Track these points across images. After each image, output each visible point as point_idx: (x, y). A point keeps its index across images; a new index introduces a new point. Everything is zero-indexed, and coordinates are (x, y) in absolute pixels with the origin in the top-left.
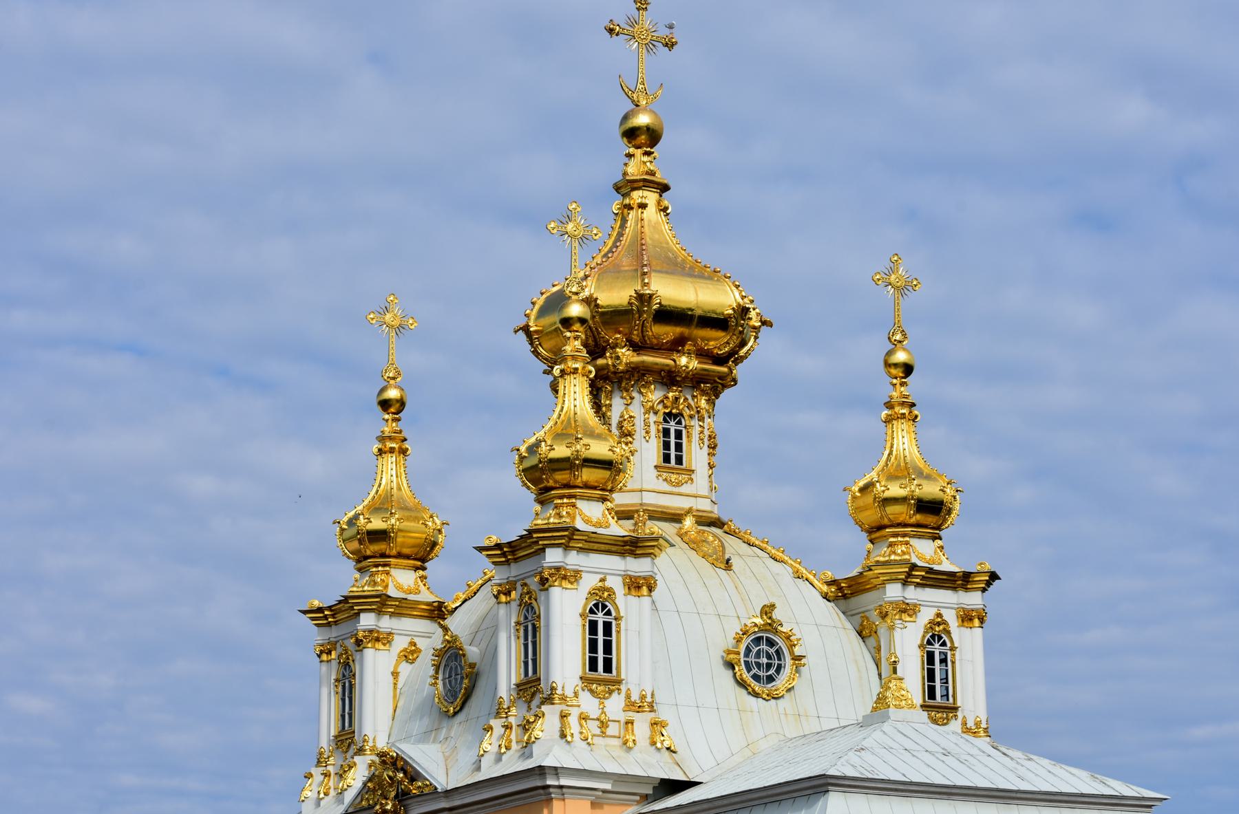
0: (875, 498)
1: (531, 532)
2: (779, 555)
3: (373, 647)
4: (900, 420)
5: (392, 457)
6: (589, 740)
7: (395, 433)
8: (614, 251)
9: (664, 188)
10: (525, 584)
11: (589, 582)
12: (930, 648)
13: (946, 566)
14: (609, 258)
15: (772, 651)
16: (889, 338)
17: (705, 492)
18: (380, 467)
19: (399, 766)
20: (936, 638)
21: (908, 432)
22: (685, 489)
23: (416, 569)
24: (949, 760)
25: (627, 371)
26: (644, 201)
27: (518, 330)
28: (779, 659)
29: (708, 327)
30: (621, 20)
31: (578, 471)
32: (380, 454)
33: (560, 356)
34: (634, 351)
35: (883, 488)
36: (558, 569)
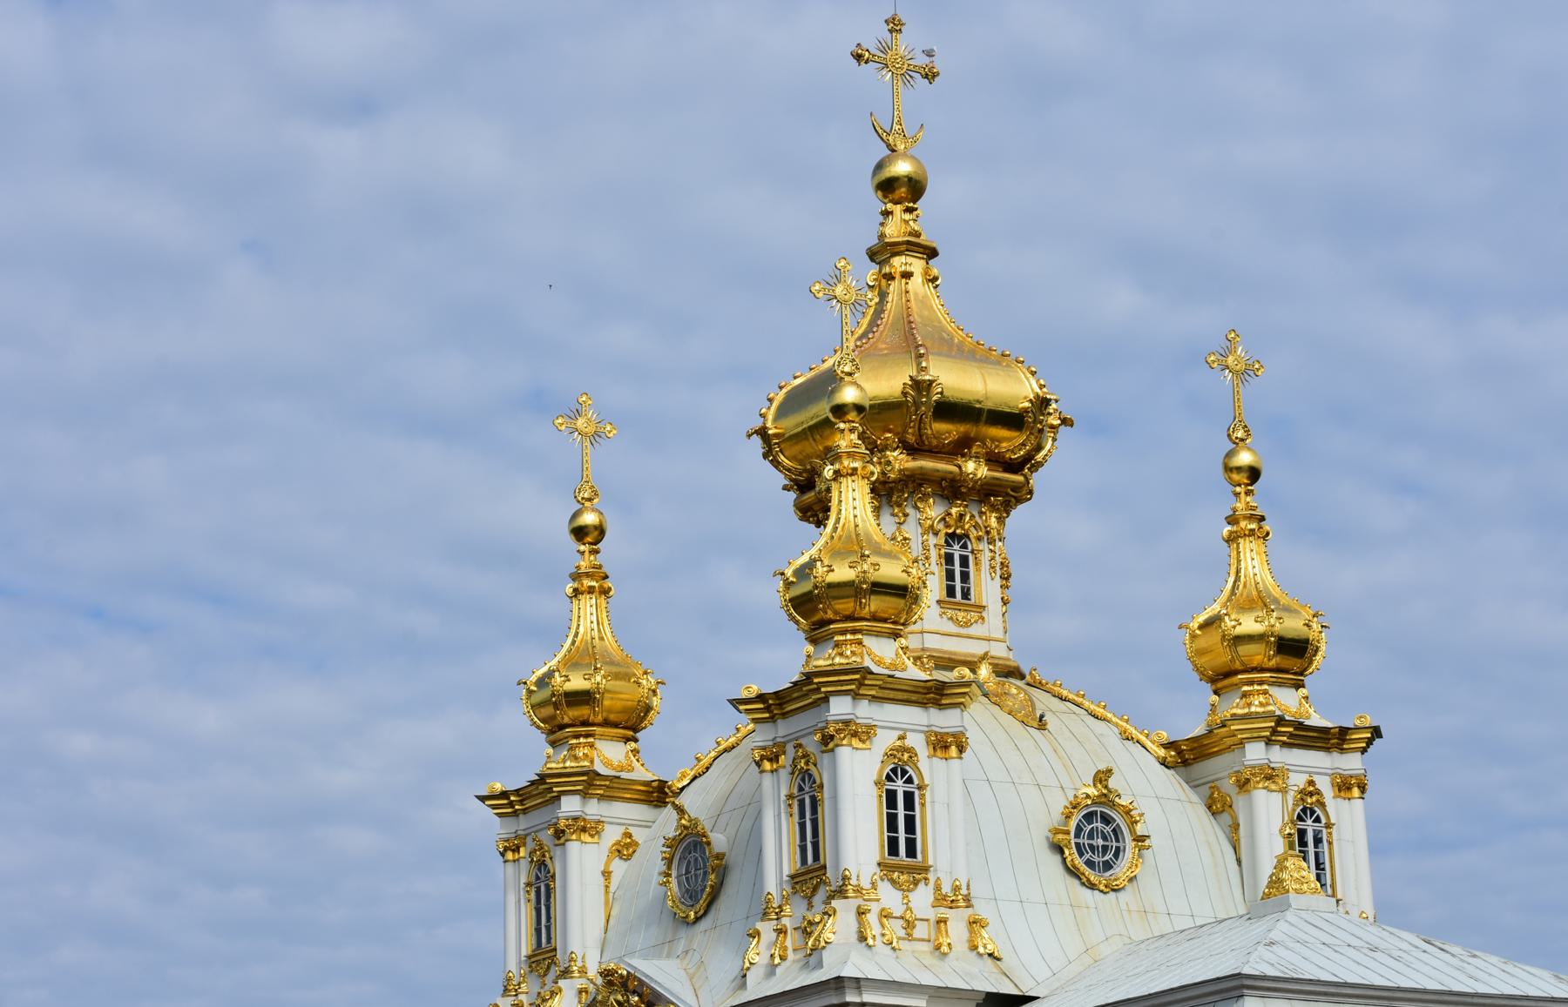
0: (1224, 636)
1: (809, 677)
2: (1100, 711)
3: (579, 839)
5: (591, 598)
6: (894, 944)
8: (875, 330)
9: (931, 253)
10: (800, 746)
11: (885, 740)
12: (1301, 825)
13: (1316, 720)
14: (869, 339)
15: (1108, 829)
16: (1229, 436)
17: (999, 634)
19: (631, 988)
20: (1306, 812)
22: (975, 630)
23: (627, 740)
24: (1378, 955)
25: (901, 480)
26: (909, 269)
27: (752, 434)
28: (1117, 840)
30: (871, 44)
31: (865, 598)
32: (575, 596)
33: (833, 453)
34: (908, 454)
35: (1233, 623)
36: (847, 723)
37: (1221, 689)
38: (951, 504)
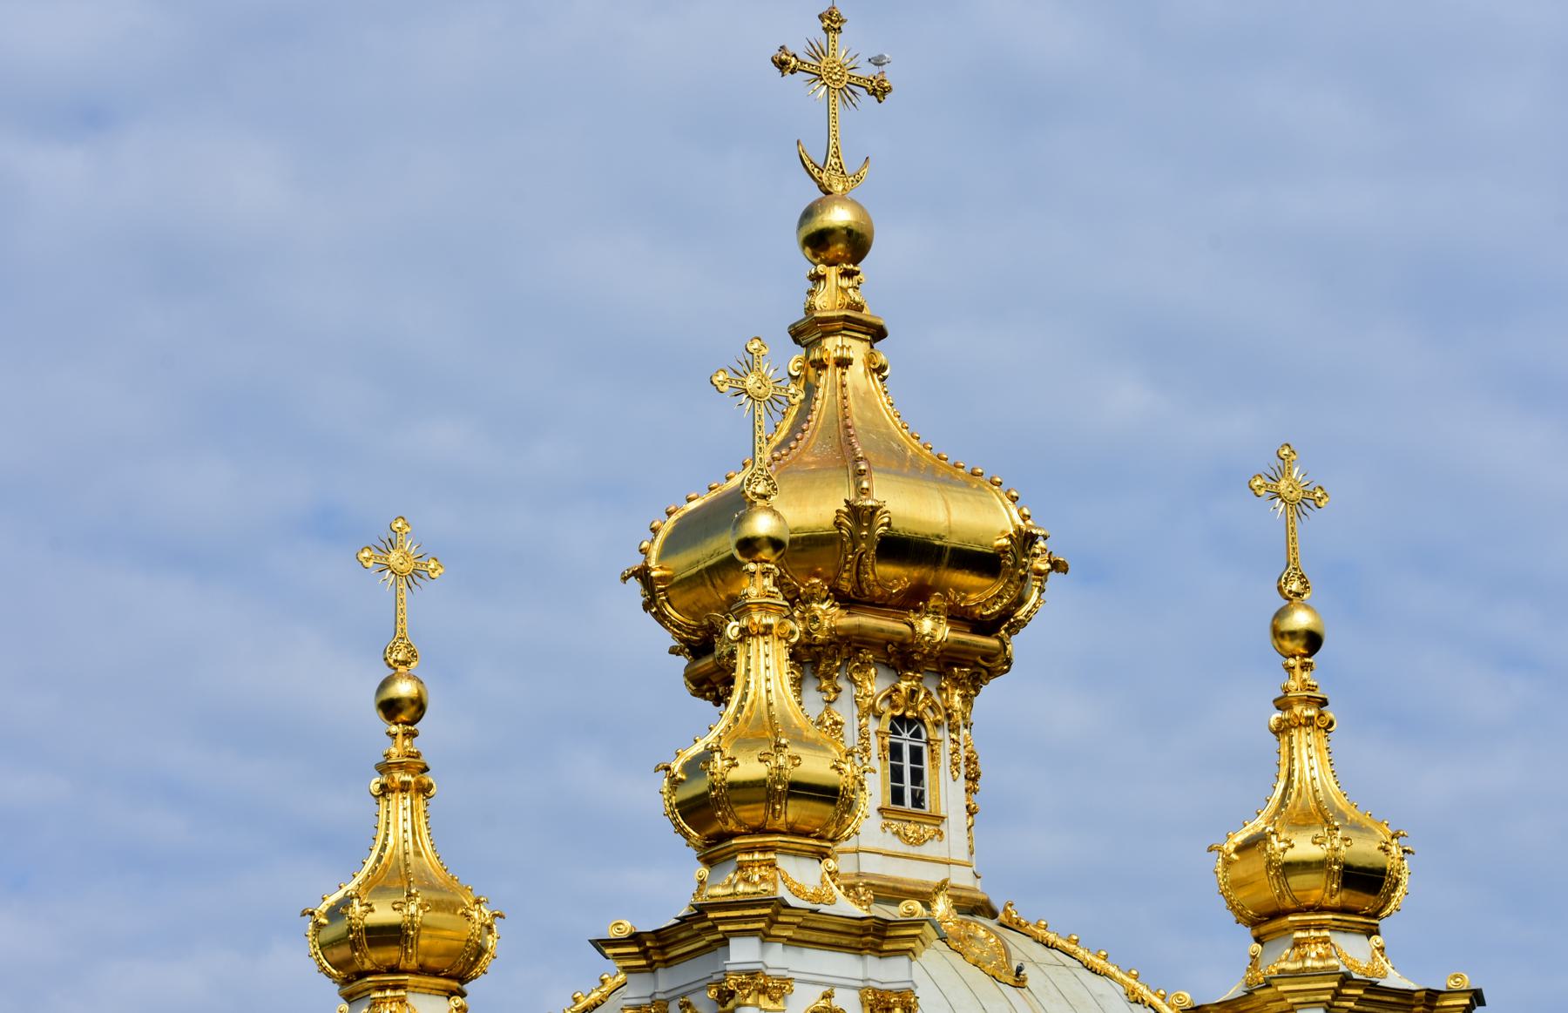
0: (1270, 863)
1: (701, 910)
2: (1099, 963)
4: (1303, 729)
5: (404, 798)
7: (408, 756)
8: (798, 437)
10: (688, 1005)
14: (791, 449)
16: (1280, 588)
17: (963, 856)
18: (383, 816)
21: (1318, 750)
22: (930, 849)
23: (451, 994)
25: (831, 643)
26: (846, 354)
27: (630, 576)
29: (967, 569)
30: (799, 48)
31: (780, 803)
32: (383, 795)
33: (739, 604)
34: (842, 608)
35: (1283, 845)
36: (752, 974)
37: (1265, 935)
38: (900, 677)
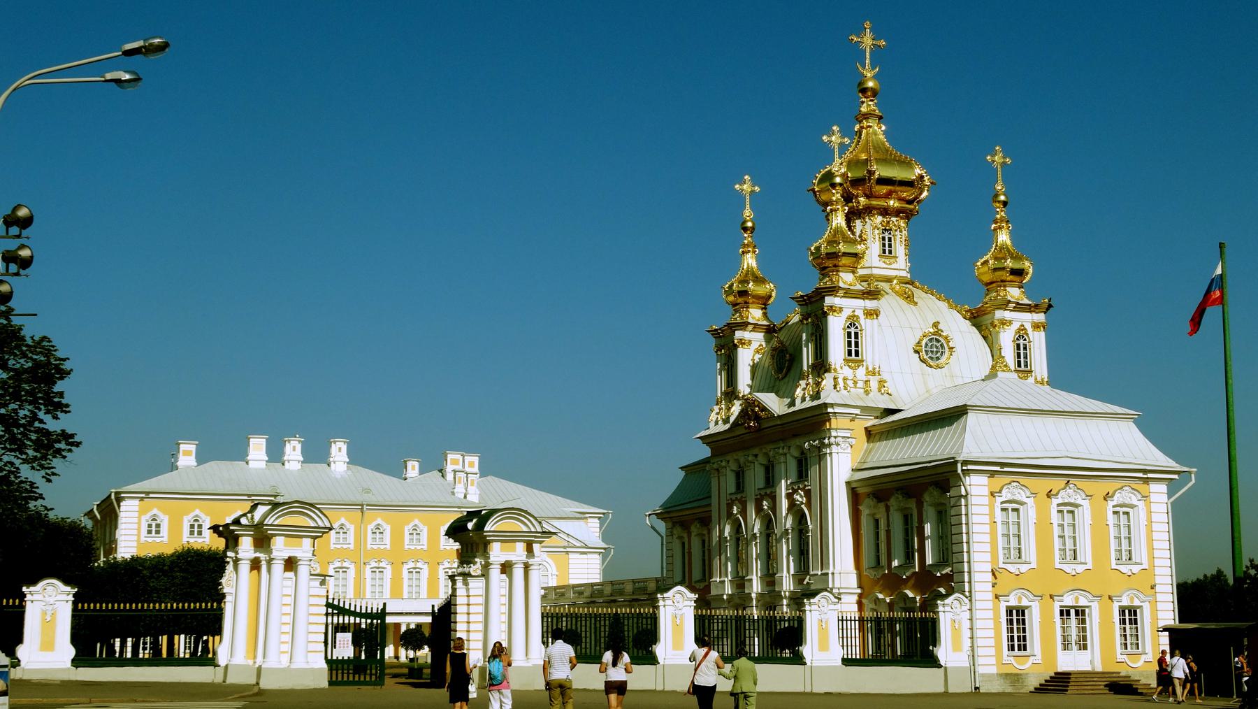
3: (742, 347)
11: (846, 313)
15: (938, 345)
20: (1021, 337)
22: (893, 266)
